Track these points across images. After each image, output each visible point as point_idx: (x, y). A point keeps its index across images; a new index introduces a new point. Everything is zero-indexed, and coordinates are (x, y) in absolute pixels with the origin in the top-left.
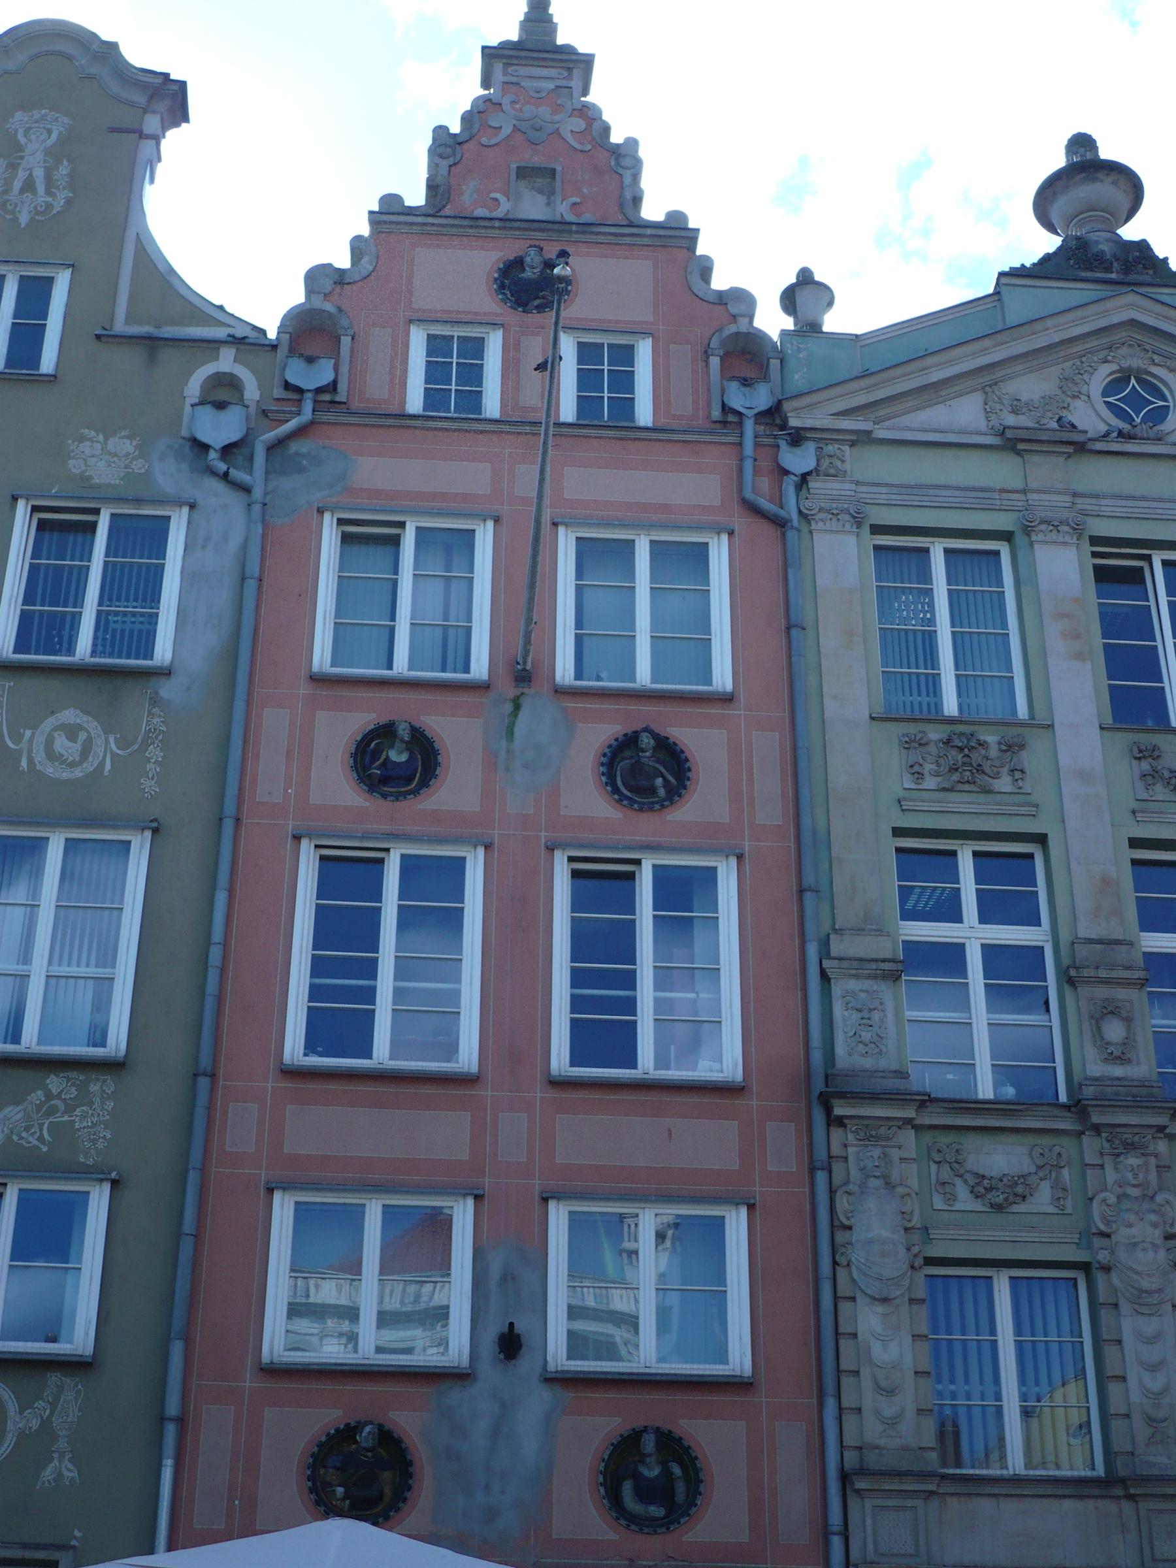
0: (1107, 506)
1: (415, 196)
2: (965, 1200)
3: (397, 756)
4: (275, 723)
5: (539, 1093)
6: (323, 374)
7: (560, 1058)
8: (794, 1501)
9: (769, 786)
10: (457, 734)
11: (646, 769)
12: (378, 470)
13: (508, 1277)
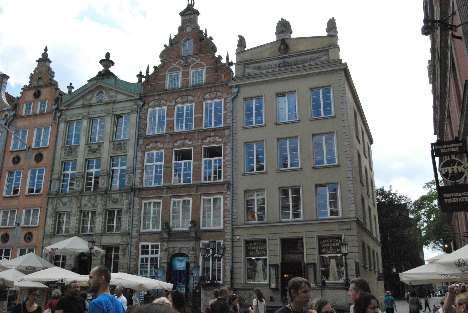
0: (92, 113)
1: (28, 84)
2: (61, 205)
3: (16, 160)
4: (6, 157)
5: (24, 197)
6: (14, 113)
7: (27, 192)
8: (41, 239)
9: (50, 158)
10: (22, 156)
11: (39, 157)
12: (20, 123)
13: (19, 217)
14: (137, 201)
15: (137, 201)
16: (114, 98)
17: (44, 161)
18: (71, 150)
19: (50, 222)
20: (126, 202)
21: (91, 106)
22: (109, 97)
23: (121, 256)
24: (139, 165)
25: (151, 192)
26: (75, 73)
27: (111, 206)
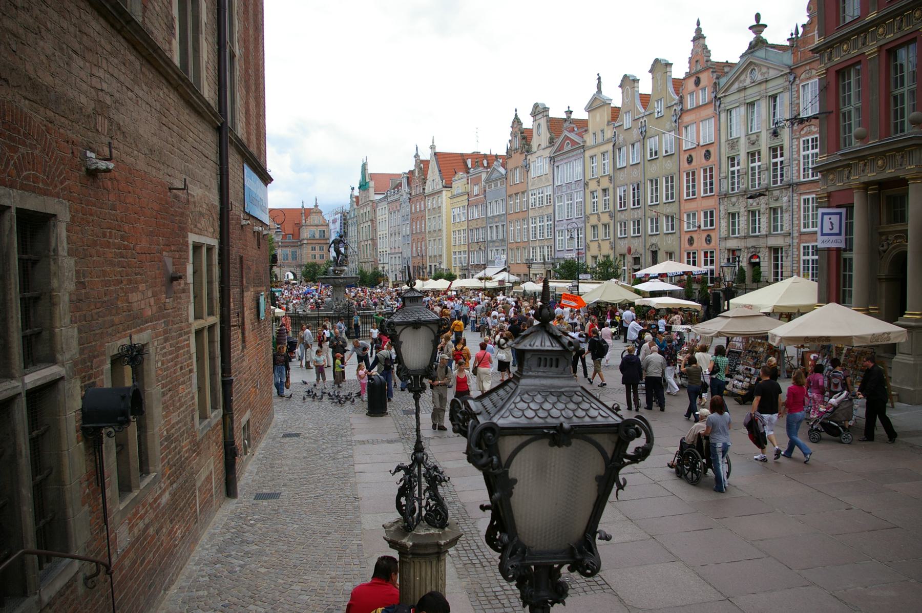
9: (717, 154)
11: (708, 155)
12: (687, 118)
14: (796, 197)
15: (796, 197)
16: (766, 76)
17: (712, 159)
18: (733, 144)
19: (723, 223)
20: (785, 199)
21: (745, 89)
22: (762, 74)
23: (784, 258)
24: (795, 156)
25: (807, 186)
26: (728, 48)
27: (773, 205)
